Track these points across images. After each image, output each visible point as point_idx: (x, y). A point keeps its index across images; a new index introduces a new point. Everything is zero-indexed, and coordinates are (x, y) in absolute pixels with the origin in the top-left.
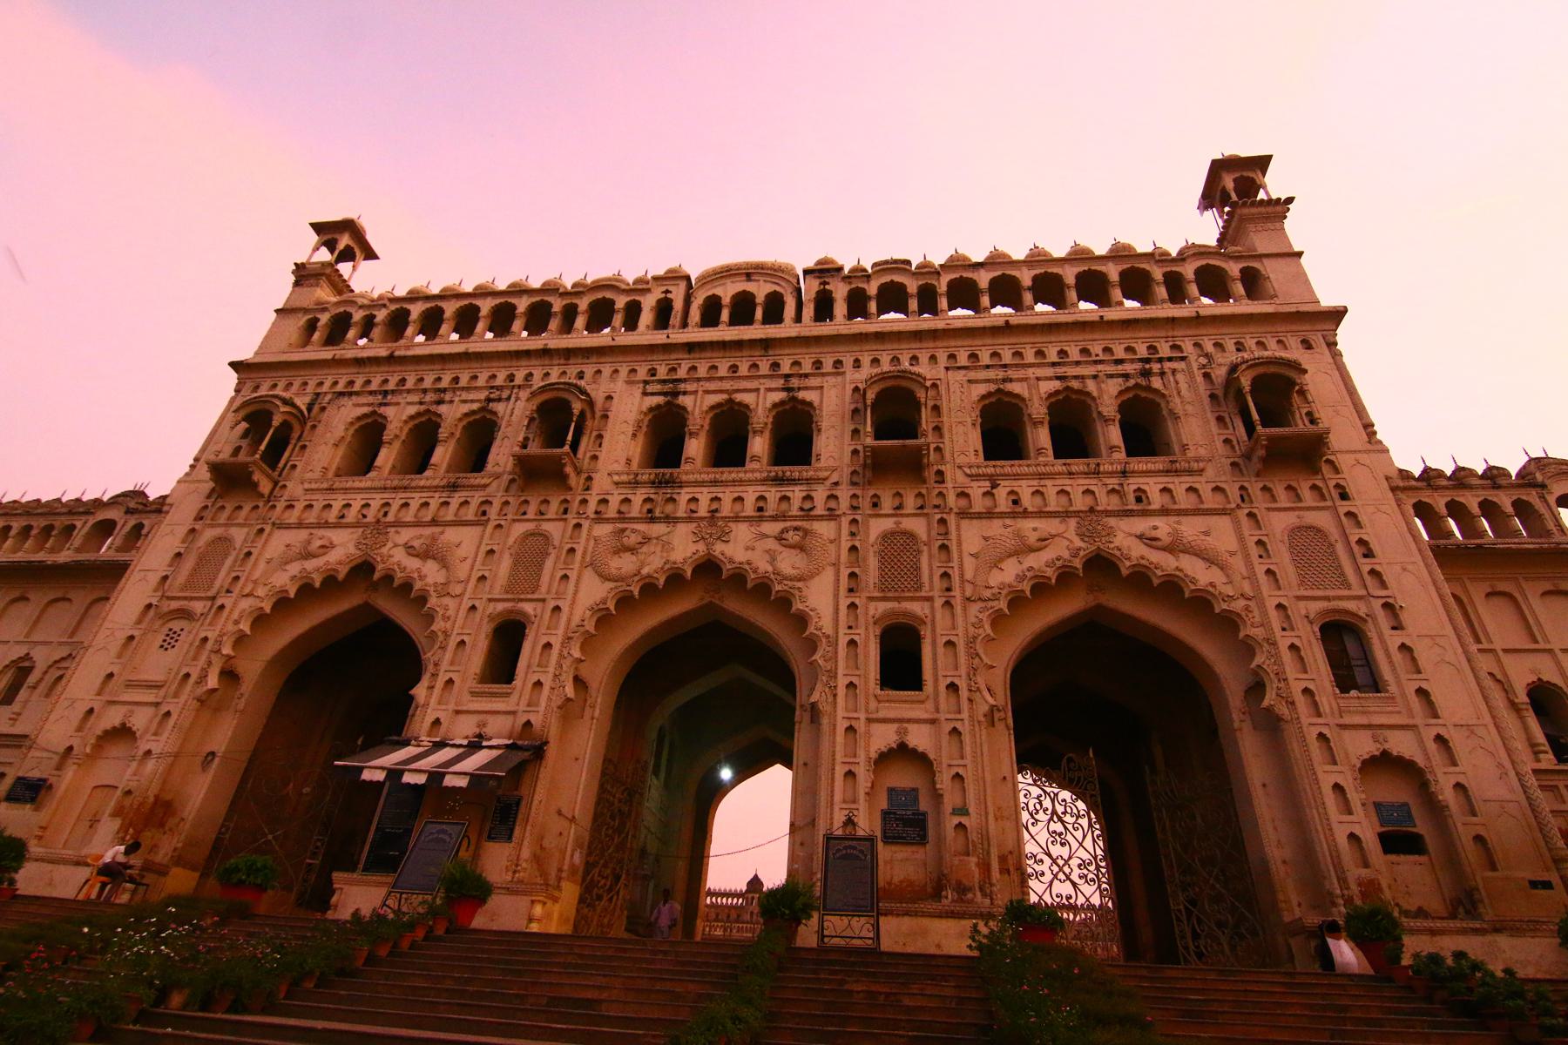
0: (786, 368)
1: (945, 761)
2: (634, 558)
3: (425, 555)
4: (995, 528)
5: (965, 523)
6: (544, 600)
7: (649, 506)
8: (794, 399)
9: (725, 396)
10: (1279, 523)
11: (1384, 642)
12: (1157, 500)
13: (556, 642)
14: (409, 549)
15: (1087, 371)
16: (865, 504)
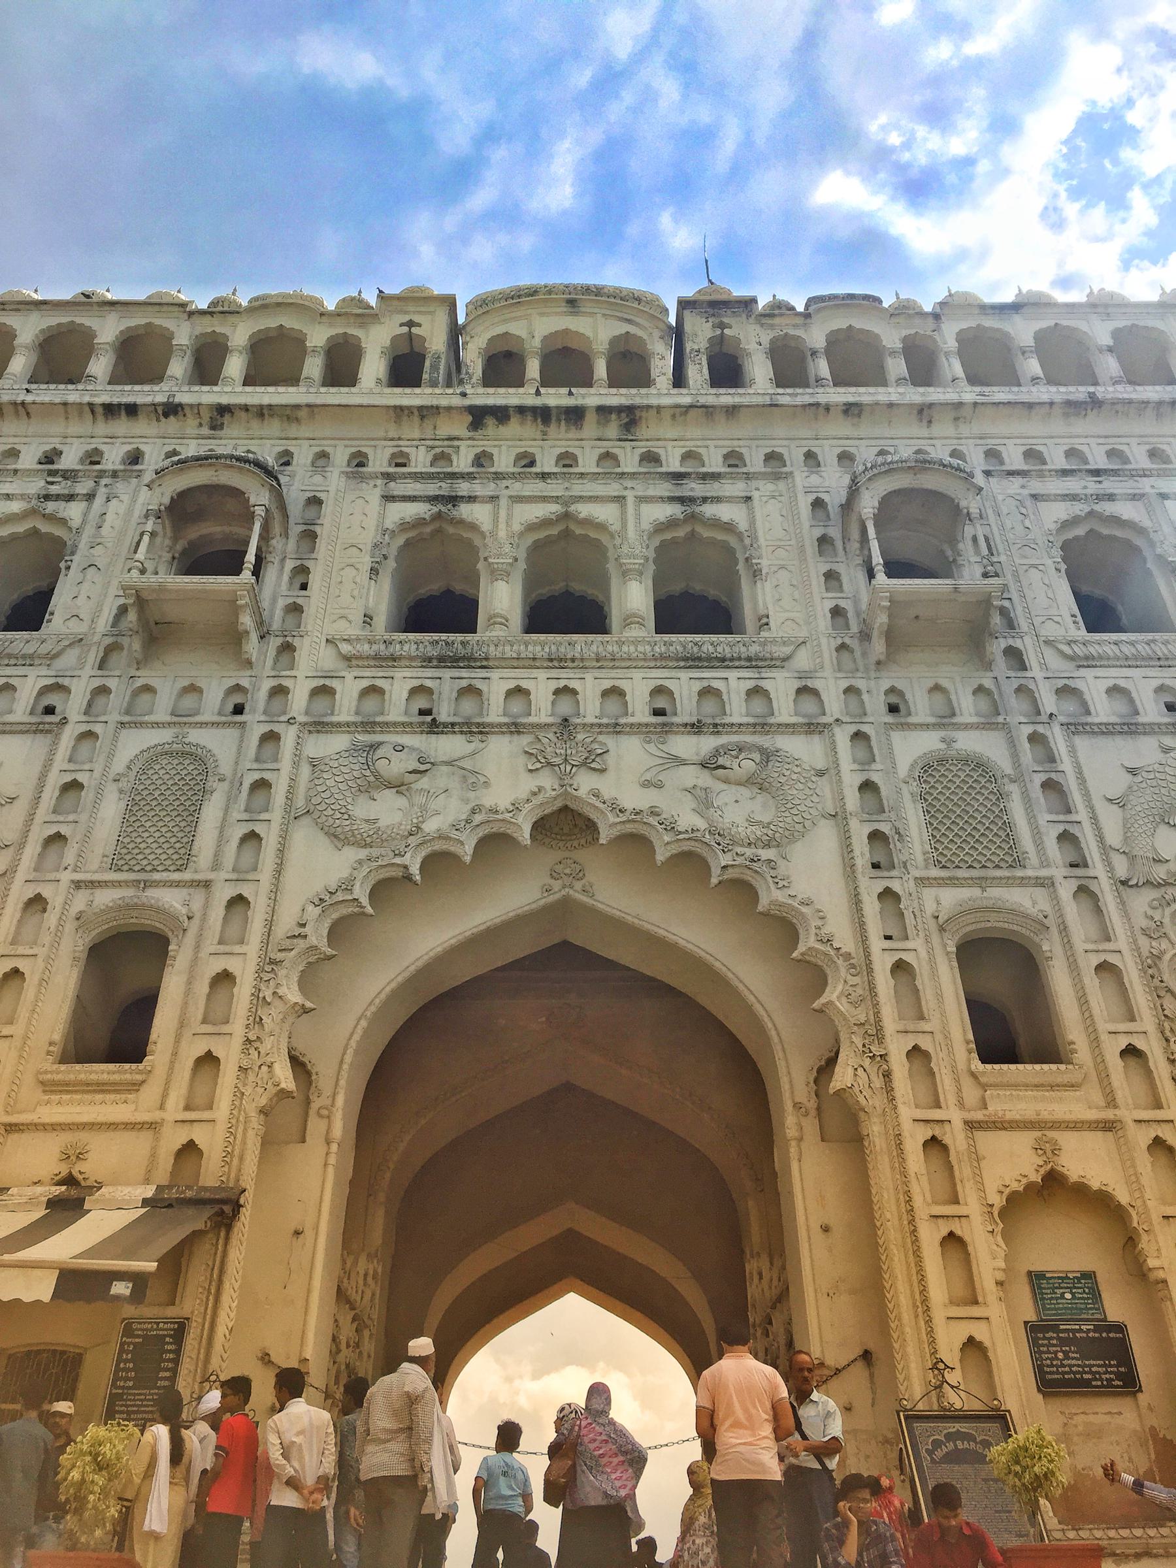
0: (673, 463)
1: (1156, 1210)
2: (402, 802)
5: (1081, 742)
6: (207, 884)
7: (422, 703)
8: (692, 517)
9: (554, 508)
13: (245, 971)
16: (876, 704)
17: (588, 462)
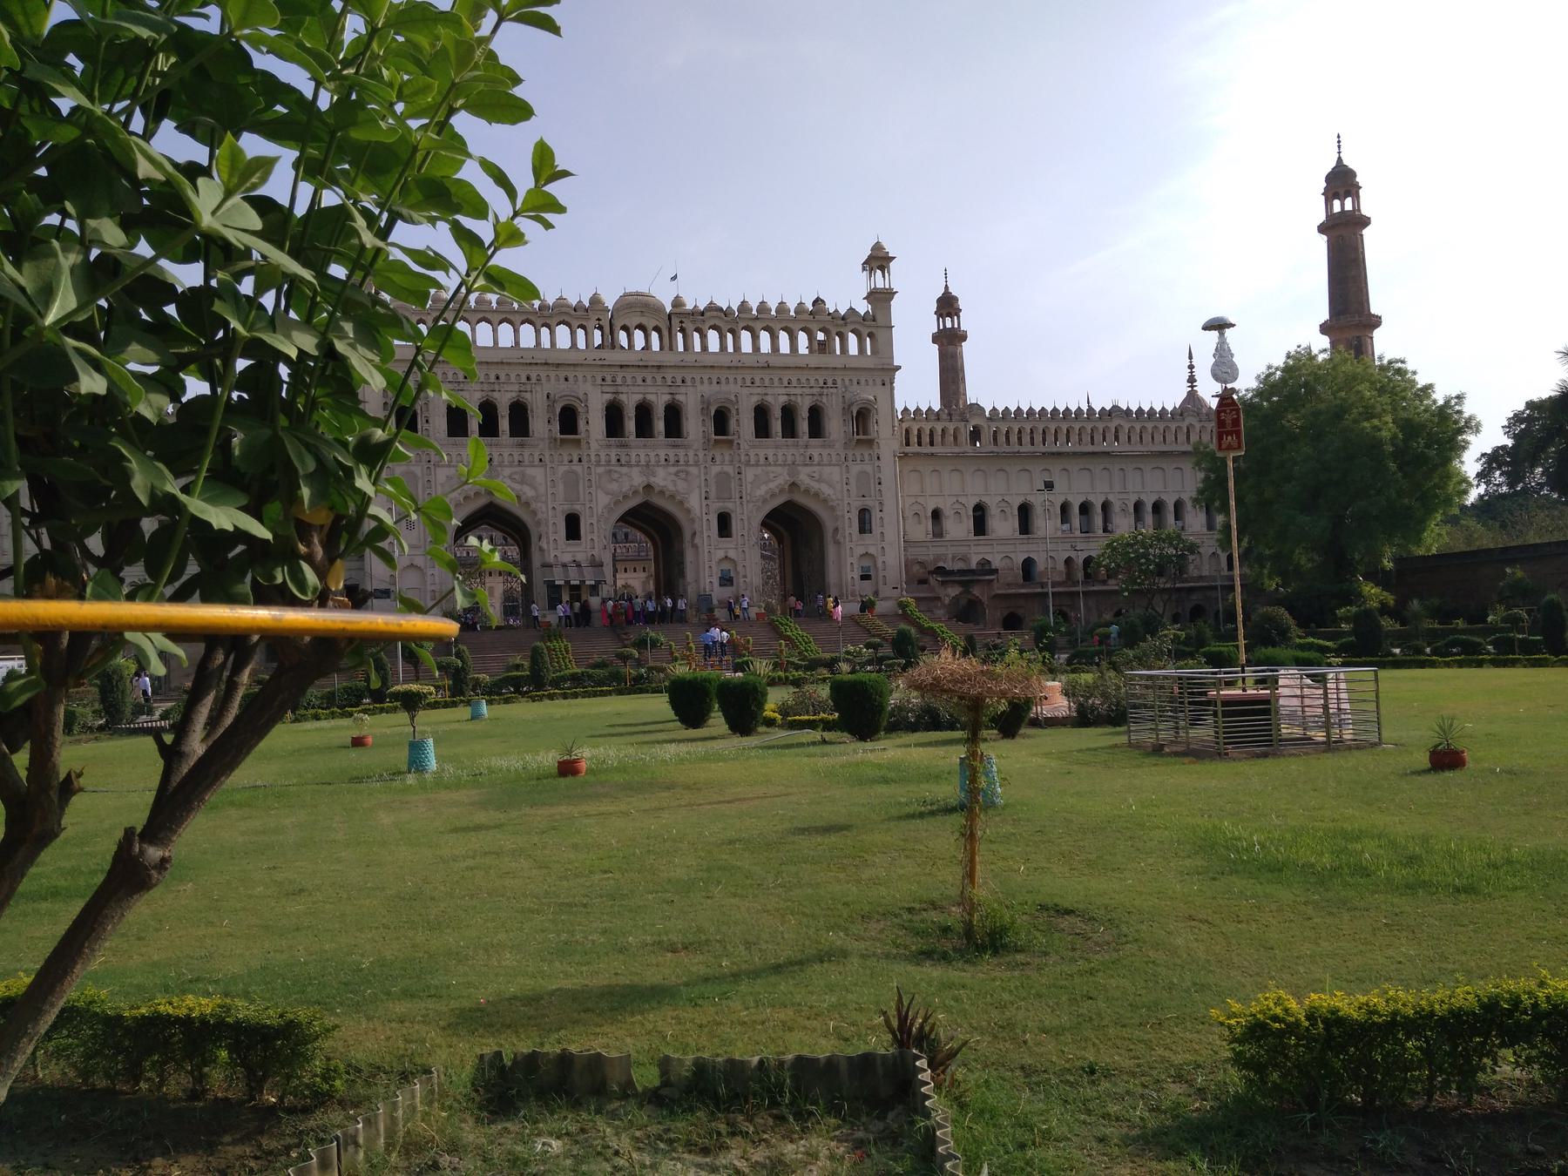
4: (759, 470)
10: (855, 469)
11: (876, 515)
12: (816, 458)
15: (798, 391)
17: (649, 381)
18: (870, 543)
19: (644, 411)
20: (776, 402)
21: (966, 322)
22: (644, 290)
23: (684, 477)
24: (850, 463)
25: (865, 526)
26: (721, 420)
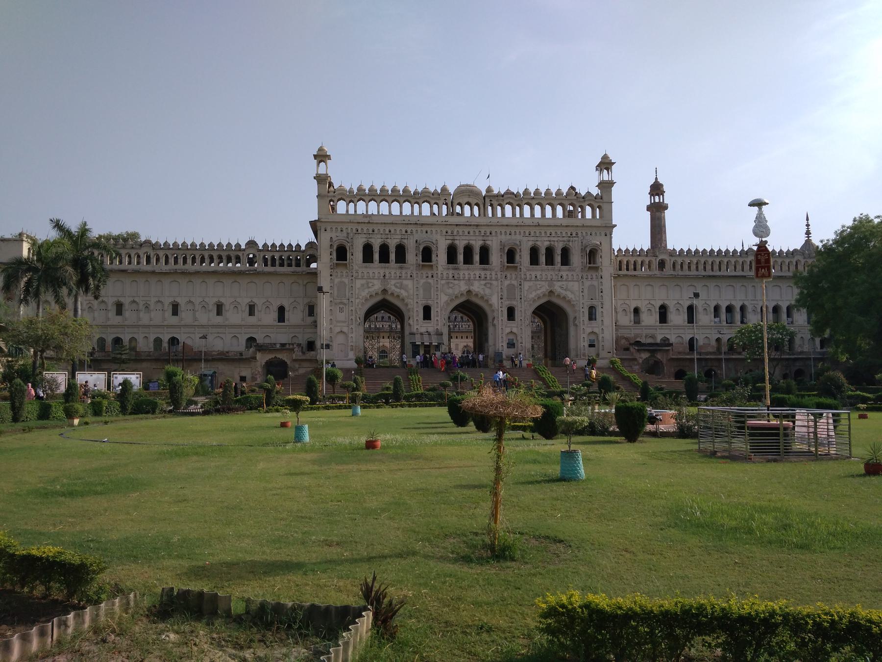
3: (400, 288)
4: (531, 283)
10: (587, 283)
11: (599, 310)
12: (565, 277)
13: (439, 310)
14: (396, 287)
15: (556, 239)
17: (472, 233)
18: (595, 326)
19: (468, 250)
20: (543, 246)
21: (668, 199)
22: (470, 183)
23: (489, 287)
24: (584, 280)
25: (592, 316)
26: (511, 256)
